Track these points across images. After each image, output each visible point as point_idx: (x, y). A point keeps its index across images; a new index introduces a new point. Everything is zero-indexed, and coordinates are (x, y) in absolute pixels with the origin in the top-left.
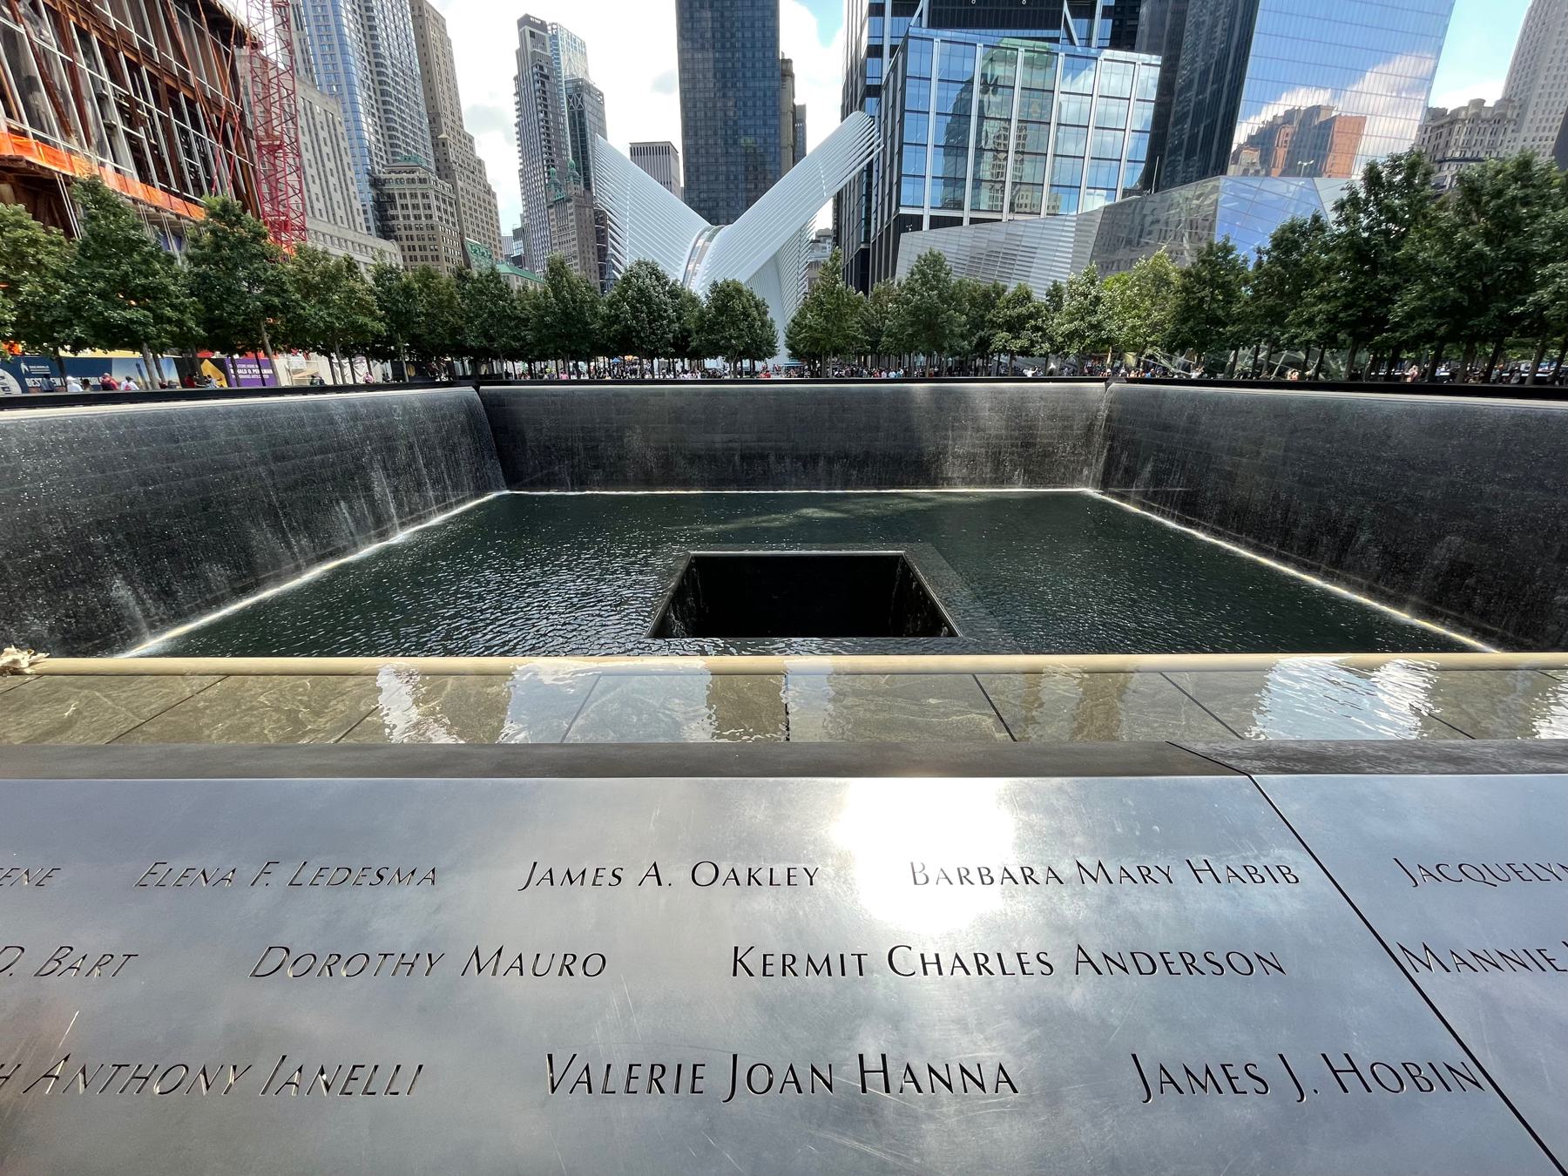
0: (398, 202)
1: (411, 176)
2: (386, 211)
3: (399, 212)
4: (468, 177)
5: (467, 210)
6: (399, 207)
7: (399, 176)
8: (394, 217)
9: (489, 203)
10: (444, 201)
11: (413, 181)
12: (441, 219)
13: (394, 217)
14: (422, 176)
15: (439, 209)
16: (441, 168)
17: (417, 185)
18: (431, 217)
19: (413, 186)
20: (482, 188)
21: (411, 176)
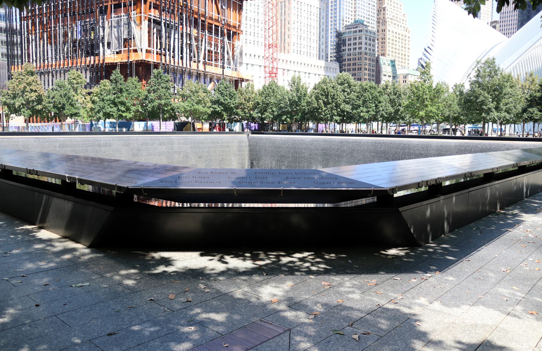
0: (347, 42)
1: (355, 29)
2: (341, 48)
3: (347, 47)
4: (395, 24)
5: (391, 41)
6: (347, 45)
7: (350, 30)
8: (344, 50)
9: (405, 36)
10: (370, 40)
11: (356, 32)
12: (366, 49)
13: (344, 50)
14: (360, 29)
15: (366, 44)
16: (381, 21)
17: (358, 33)
18: (360, 48)
19: (355, 34)
20: (403, 28)
21: (355, 29)
